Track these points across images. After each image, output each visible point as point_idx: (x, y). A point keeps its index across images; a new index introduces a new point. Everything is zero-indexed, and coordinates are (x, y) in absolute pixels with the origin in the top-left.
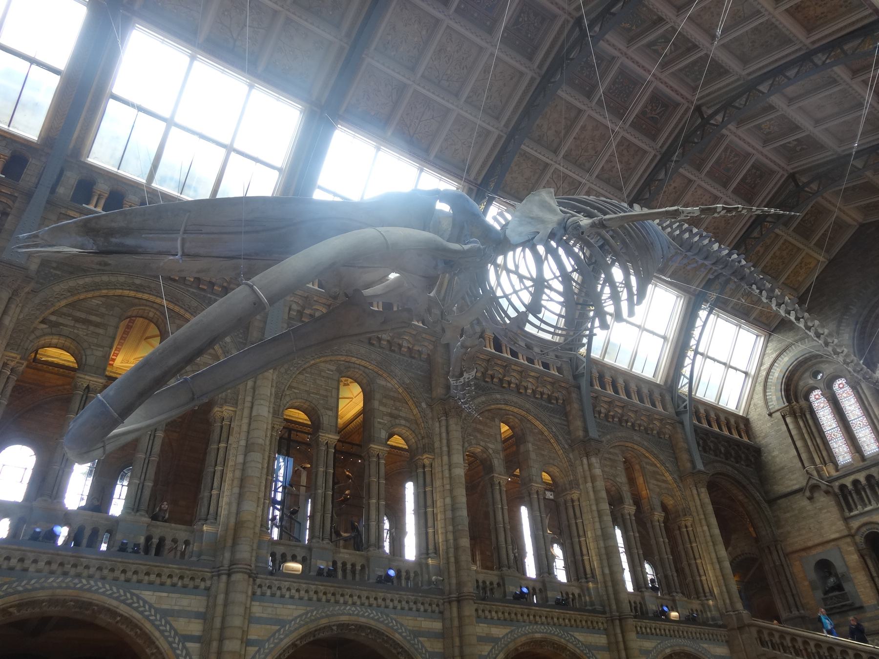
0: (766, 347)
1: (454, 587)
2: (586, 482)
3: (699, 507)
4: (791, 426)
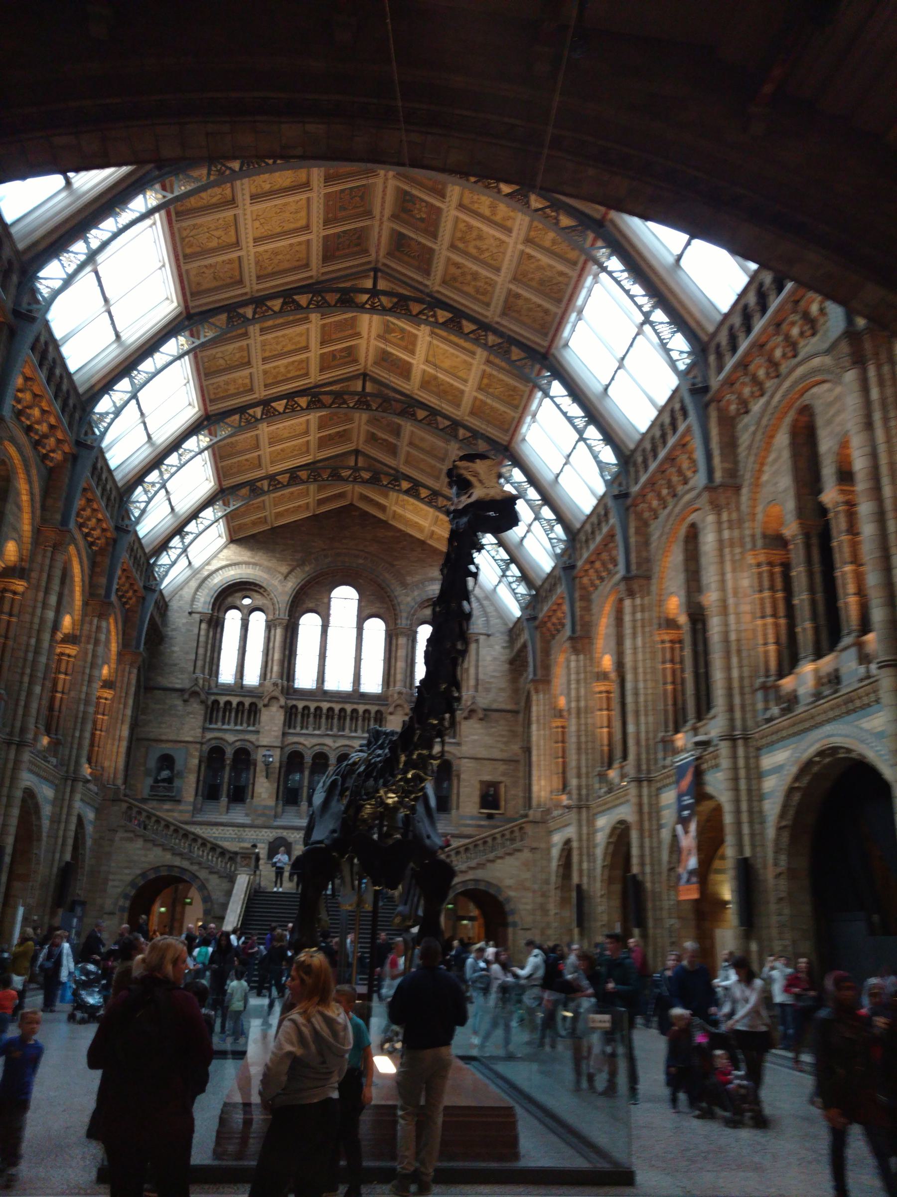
0: (221, 551)
2: (88, 643)
4: (203, 633)
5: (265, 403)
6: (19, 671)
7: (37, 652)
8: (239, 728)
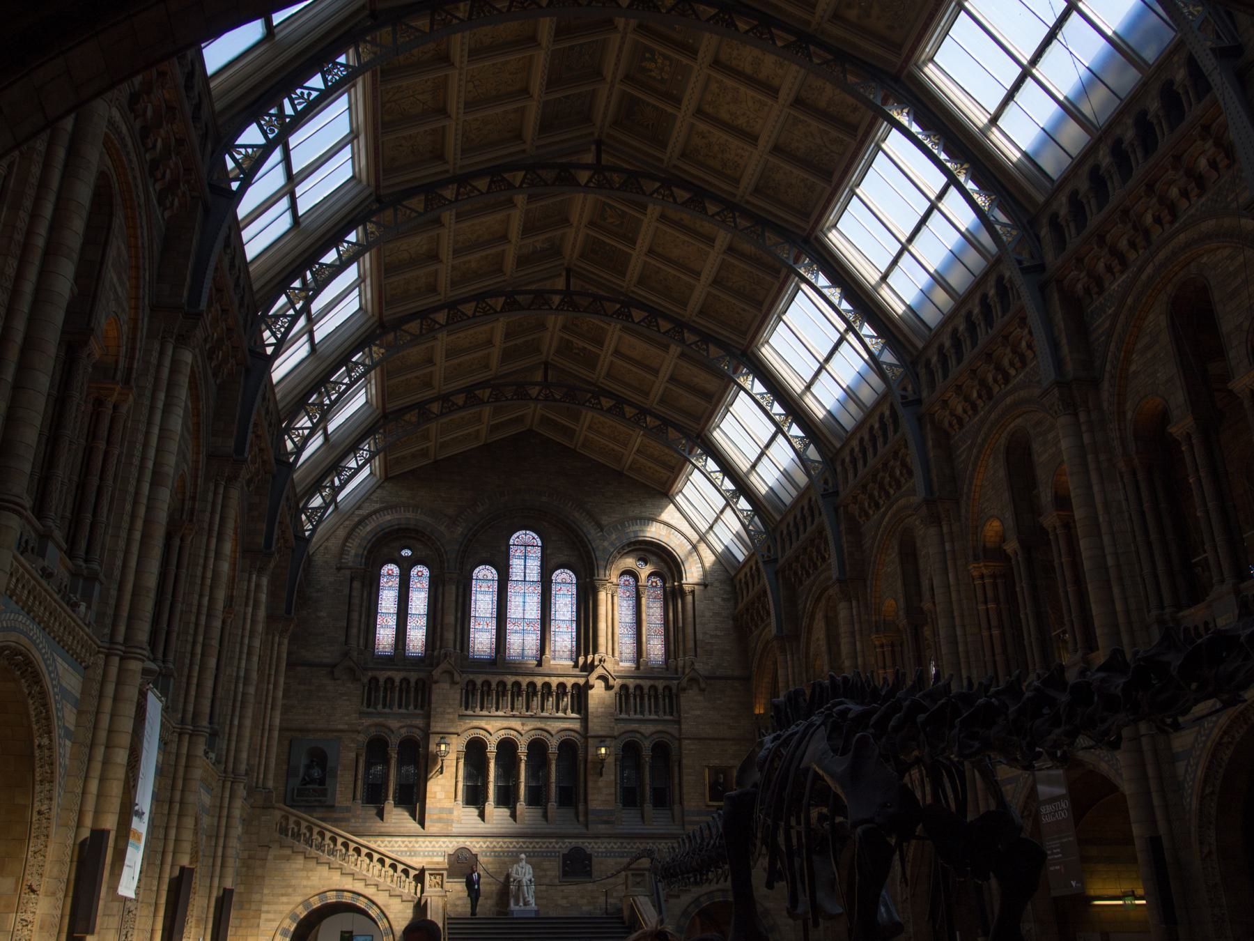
0: (374, 491)
1: (190, 716)
2: (246, 605)
3: (275, 660)
4: (355, 593)
5: (452, 306)
6: (190, 639)
7: (210, 616)
8: (403, 711)
